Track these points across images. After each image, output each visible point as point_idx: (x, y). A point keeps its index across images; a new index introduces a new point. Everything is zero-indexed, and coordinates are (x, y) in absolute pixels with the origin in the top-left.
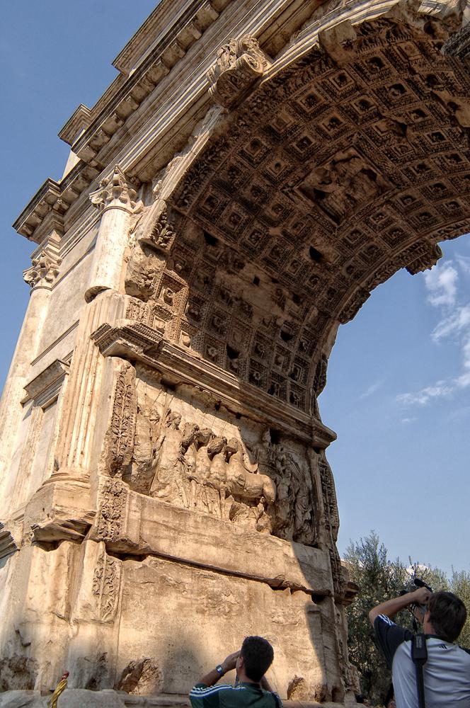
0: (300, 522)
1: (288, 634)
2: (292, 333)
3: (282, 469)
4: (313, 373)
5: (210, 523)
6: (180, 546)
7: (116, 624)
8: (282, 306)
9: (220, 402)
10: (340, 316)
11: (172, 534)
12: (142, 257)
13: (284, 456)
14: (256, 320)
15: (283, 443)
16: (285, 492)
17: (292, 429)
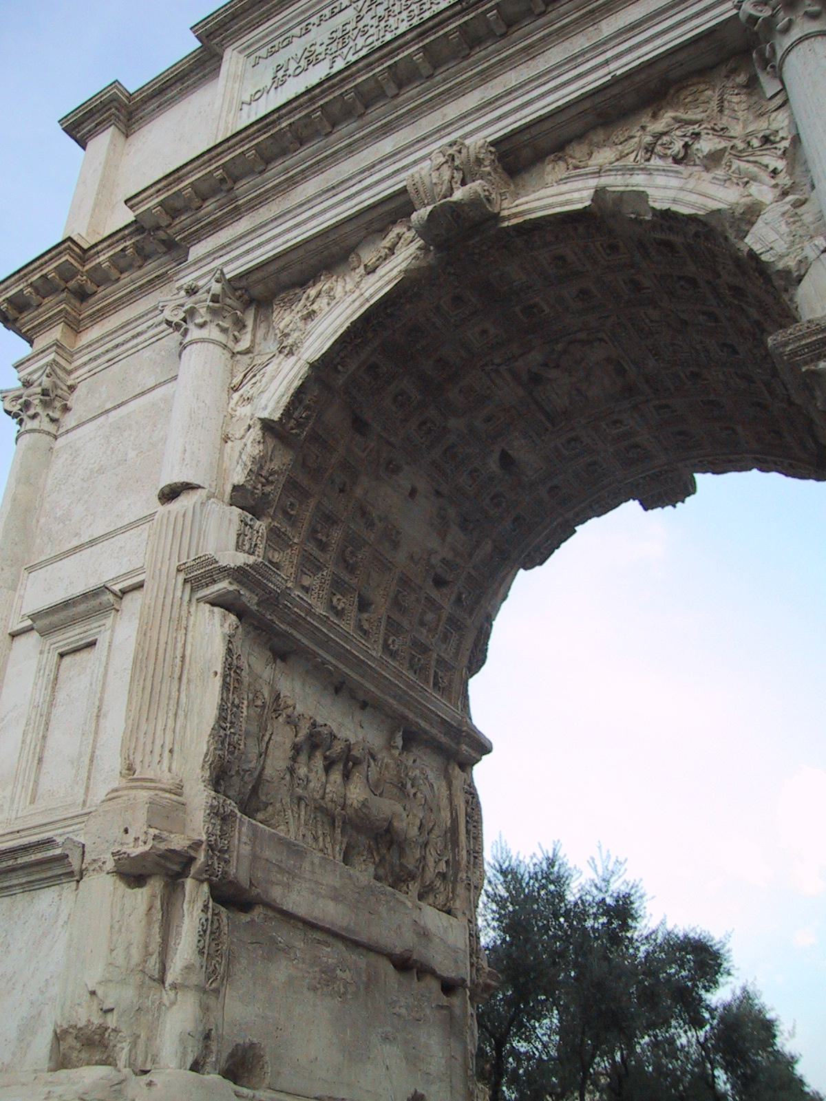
0: (430, 874)
1: (410, 1033)
2: (449, 577)
3: (413, 791)
4: (468, 643)
5: (329, 868)
6: (294, 896)
7: (222, 994)
8: (443, 535)
9: (344, 683)
10: (524, 559)
11: (285, 879)
12: (261, 447)
13: (417, 772)
14: (401, 557)
15: (417, 751)
16: (416, 829)
17: (434, 731)
